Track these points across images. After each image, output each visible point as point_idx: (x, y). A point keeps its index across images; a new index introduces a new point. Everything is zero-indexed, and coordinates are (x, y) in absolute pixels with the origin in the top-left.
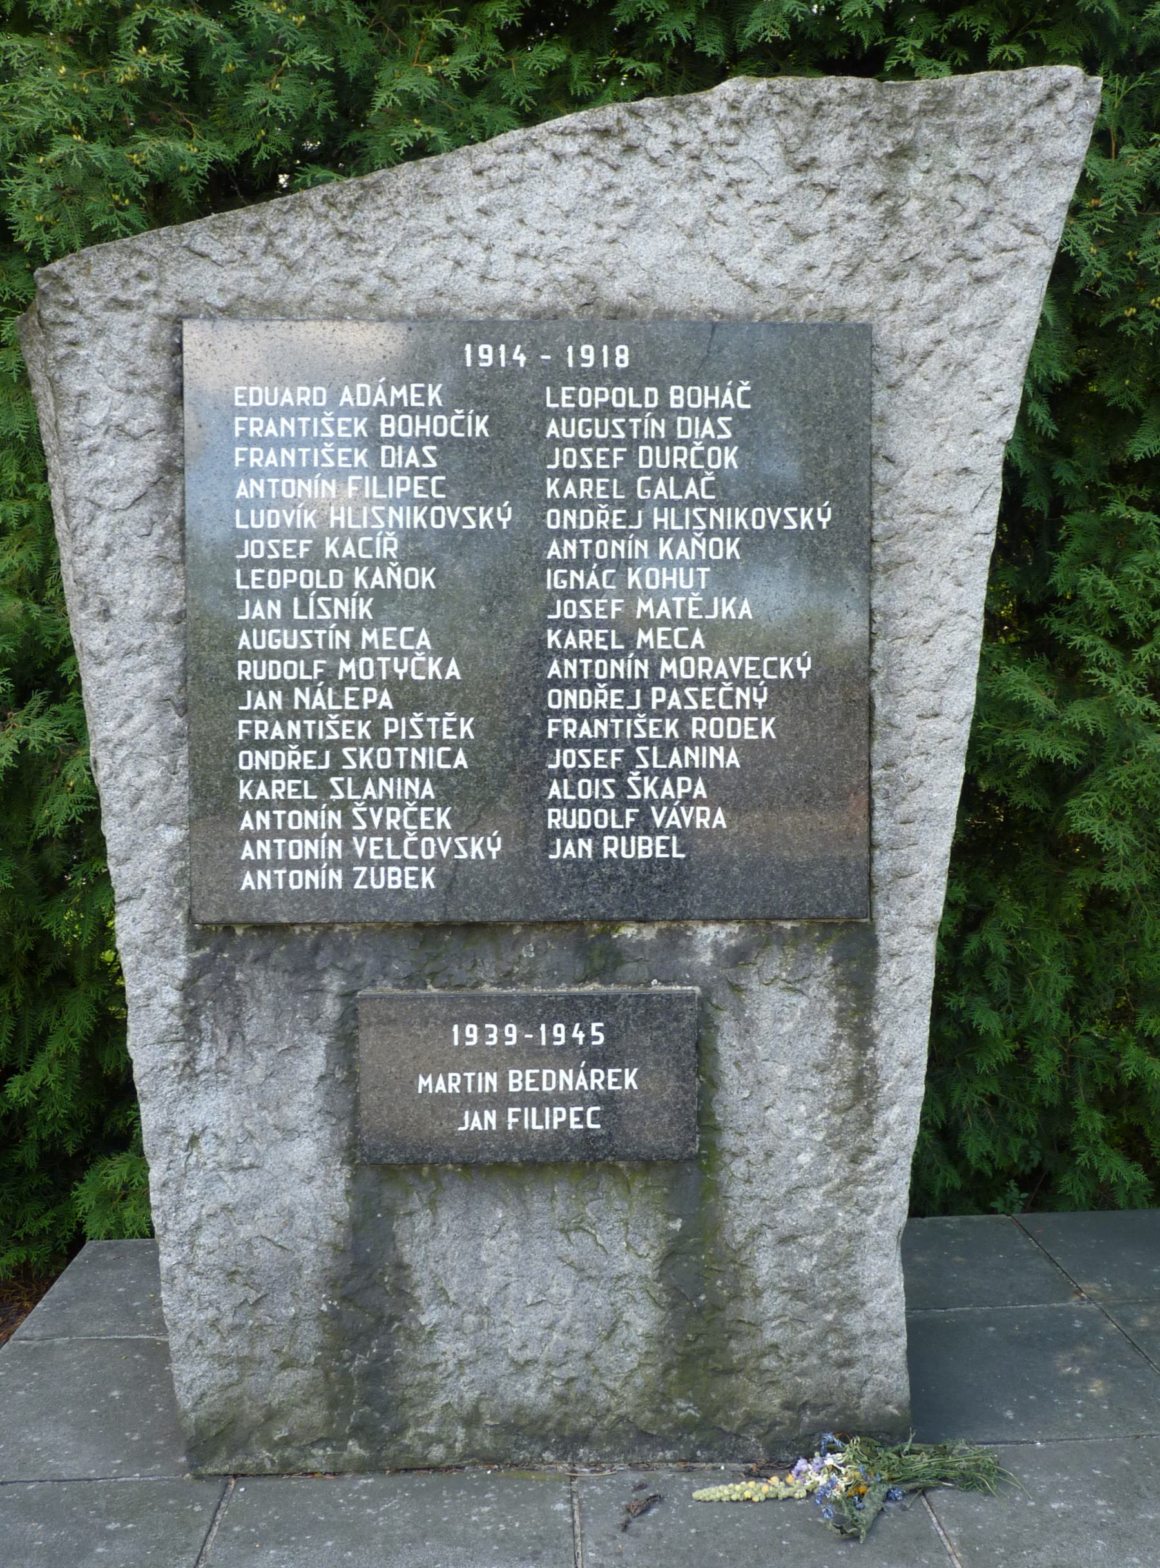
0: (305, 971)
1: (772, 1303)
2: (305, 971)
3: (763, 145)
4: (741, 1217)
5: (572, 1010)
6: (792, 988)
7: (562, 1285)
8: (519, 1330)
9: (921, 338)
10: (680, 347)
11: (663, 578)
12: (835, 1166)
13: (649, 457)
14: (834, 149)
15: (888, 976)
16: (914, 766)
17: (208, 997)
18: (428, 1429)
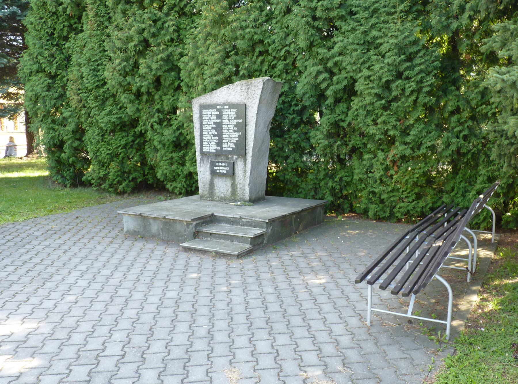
0: (208, 158)
1: (239, 189)
2: (208, 158)
3: (239, 88)
4: (237, 182)
5: (224, 162)
6: (241, 161)
7: (225, 186)
8: (222, 190)
9: (250, 105)
10: (232, 106)
11: (230, 126)
12: (243, 178)
13: (230, 116)
14: (244, 88)
15: (247, 161)
16: (249, 143)
17: (202, 159)
18: (215, 198)
